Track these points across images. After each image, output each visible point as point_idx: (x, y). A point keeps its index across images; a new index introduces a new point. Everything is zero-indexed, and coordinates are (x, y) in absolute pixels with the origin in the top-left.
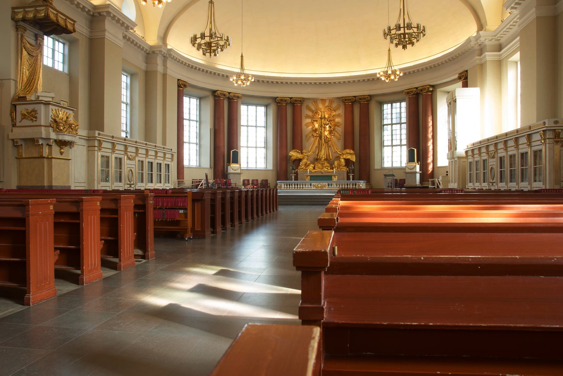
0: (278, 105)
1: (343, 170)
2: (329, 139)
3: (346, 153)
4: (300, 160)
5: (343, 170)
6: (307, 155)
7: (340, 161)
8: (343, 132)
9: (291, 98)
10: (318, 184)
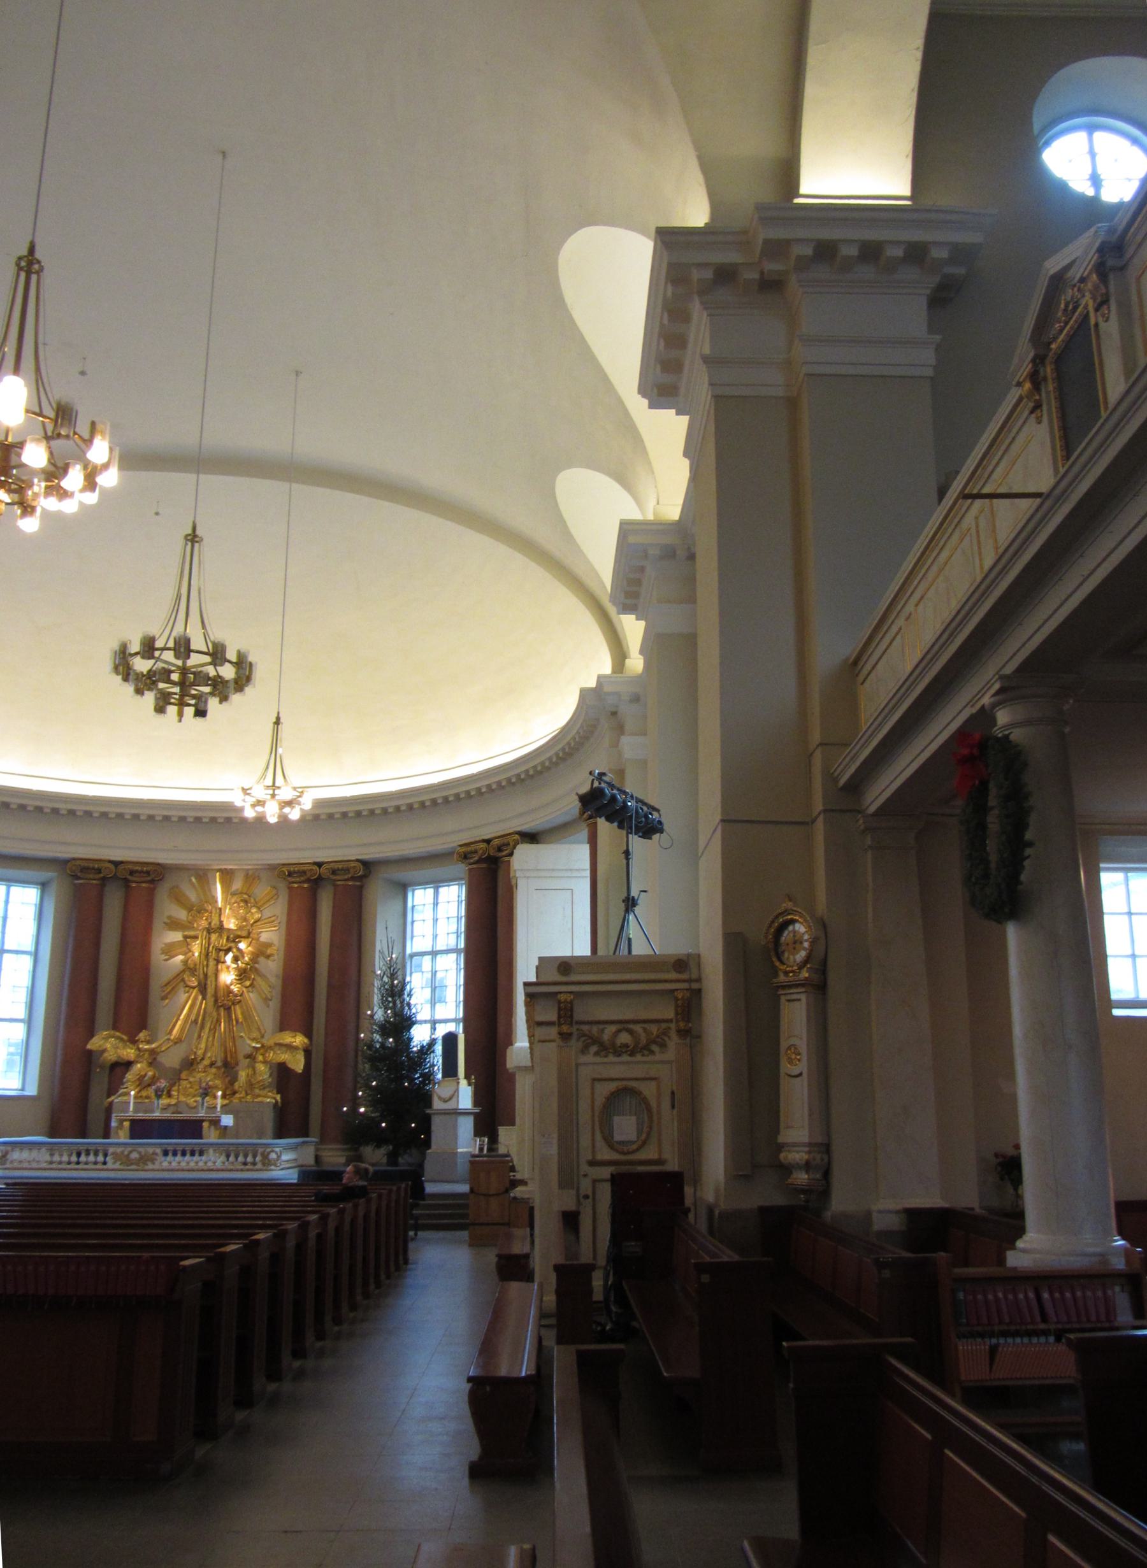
0: (75, 885)
1: (260, 1099)
2: (236, 996)
3: (276, 1044)
4: (128, 1064)
5: (260, 1099)
6: (153, 1052)
7: (254, 1068)
8: (281, 972)
9: (117, 864)
10: (131, 1152)
